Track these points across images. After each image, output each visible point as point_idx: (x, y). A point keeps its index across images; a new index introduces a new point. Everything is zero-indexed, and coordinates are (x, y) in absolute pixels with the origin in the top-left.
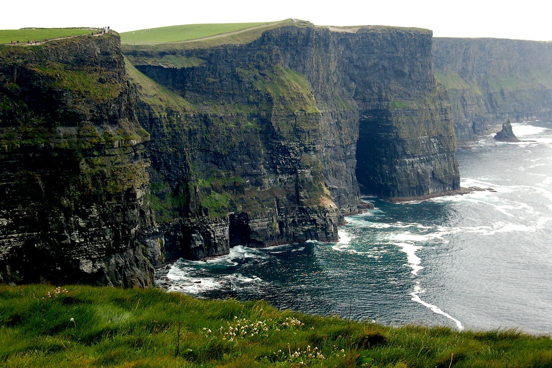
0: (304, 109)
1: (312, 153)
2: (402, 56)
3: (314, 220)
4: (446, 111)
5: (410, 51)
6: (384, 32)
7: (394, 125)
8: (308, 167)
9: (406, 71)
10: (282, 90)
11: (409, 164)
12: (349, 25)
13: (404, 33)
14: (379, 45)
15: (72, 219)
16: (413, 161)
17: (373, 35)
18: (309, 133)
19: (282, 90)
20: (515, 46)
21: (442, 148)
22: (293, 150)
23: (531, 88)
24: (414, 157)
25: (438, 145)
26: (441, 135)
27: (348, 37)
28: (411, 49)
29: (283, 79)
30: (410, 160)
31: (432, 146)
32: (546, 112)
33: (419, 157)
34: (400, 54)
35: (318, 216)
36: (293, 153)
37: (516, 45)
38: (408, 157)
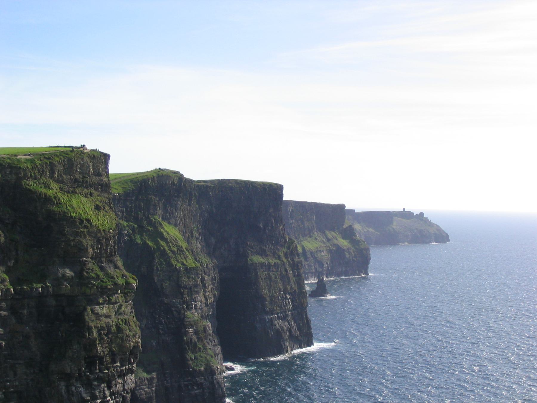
0: (185, 262)
1: (193, 311)
3: (202, 384)
4: (298, 266)
8: (192, 327)
10: (163, 243)
11: (268, 322)
12: (204, 179)
15: (74, 389)
17: (231, 188)
18: (191, 288)
19: (163, 243)
22: (176, 307)
29: (162, 230)
30: (269, 317)
31: (287, 302)
33: (277, 314)
35: (205, 379)
36: (175, 310)
38: (267, 313)
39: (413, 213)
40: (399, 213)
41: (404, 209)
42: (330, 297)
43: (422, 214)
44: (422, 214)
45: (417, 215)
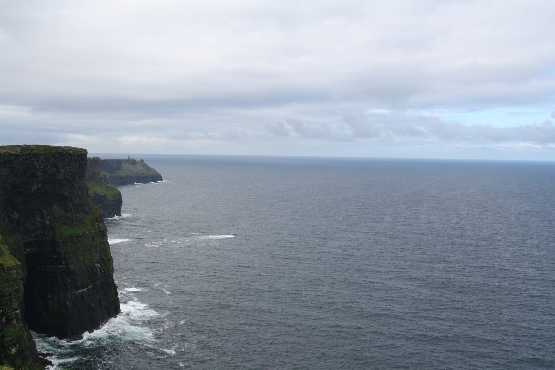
2: (63, 178)
5: (71, 173)
6: (46, 152)
9: (67, 194)
13: (65, 153)
14: (42, 167)
16: (83, 292)
17: (36, 155)
21: (104, 272)
24: (83, 288)
25: (100, 269)
27: (12, 159)
34: (60, 177)
40: (125, 160)
43: (142, 161)
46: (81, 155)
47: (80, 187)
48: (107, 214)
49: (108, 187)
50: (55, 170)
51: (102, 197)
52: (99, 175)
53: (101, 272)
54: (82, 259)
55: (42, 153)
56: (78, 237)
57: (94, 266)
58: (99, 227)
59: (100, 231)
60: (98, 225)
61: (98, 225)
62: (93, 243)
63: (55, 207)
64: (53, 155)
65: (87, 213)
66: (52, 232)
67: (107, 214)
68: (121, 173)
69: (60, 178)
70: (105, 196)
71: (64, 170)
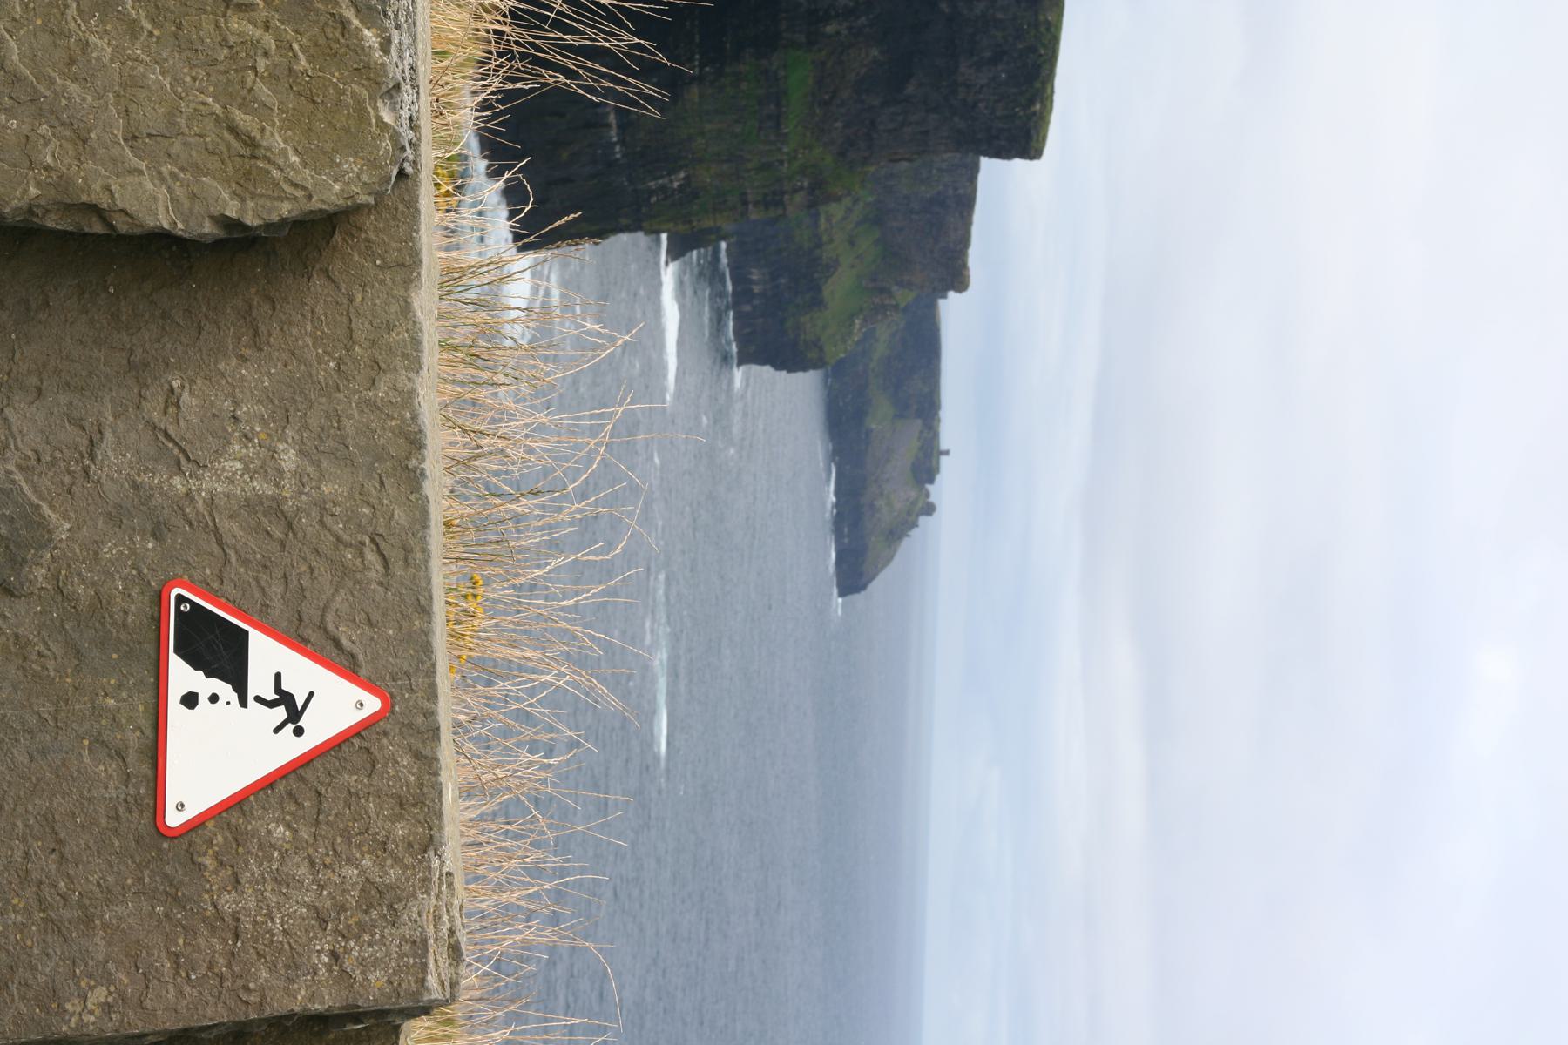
5: (975, 105)
6: (1042, 29)
7: (728, 70)
9: (910, 89)
13: (1038, 85)
14: (1000, 15)
16: (608, 126)
20: (956, 189)
21: (654, 199)
23: (825, 238)
24: (619, 127)
25: (663, 188)
26: (695, 195)
28: (981, 105)
32: (752, 282)
37: (961, 191)
39: (931, 481)
41: (947, 453)
42: (669, 275)
43: (929, 509)
44: (929, 509)
45: (928, 495)
46: (1028, 136)
47: (926, 133)
48: (747, 308)
49: (851, 317)
50: (988, 54)
51: (819, 290)
52: (901, 284)
53: (651, 192)
54: (708, 127)
55: (1041, 18)
56: (777, 120)
57: (681, 168)
58: (795, 191)
59: (783, 193)
60: (802, 188)
61: (802, 188)
62: (749, 165)
63: (875, 52)
64: (1033, 49)
65: (842, 154)
66: (802, 38)
67: (747, 308)
68: (880, 417)
69: (962, 69)
70: (817, 303)
71: (984, 81)
